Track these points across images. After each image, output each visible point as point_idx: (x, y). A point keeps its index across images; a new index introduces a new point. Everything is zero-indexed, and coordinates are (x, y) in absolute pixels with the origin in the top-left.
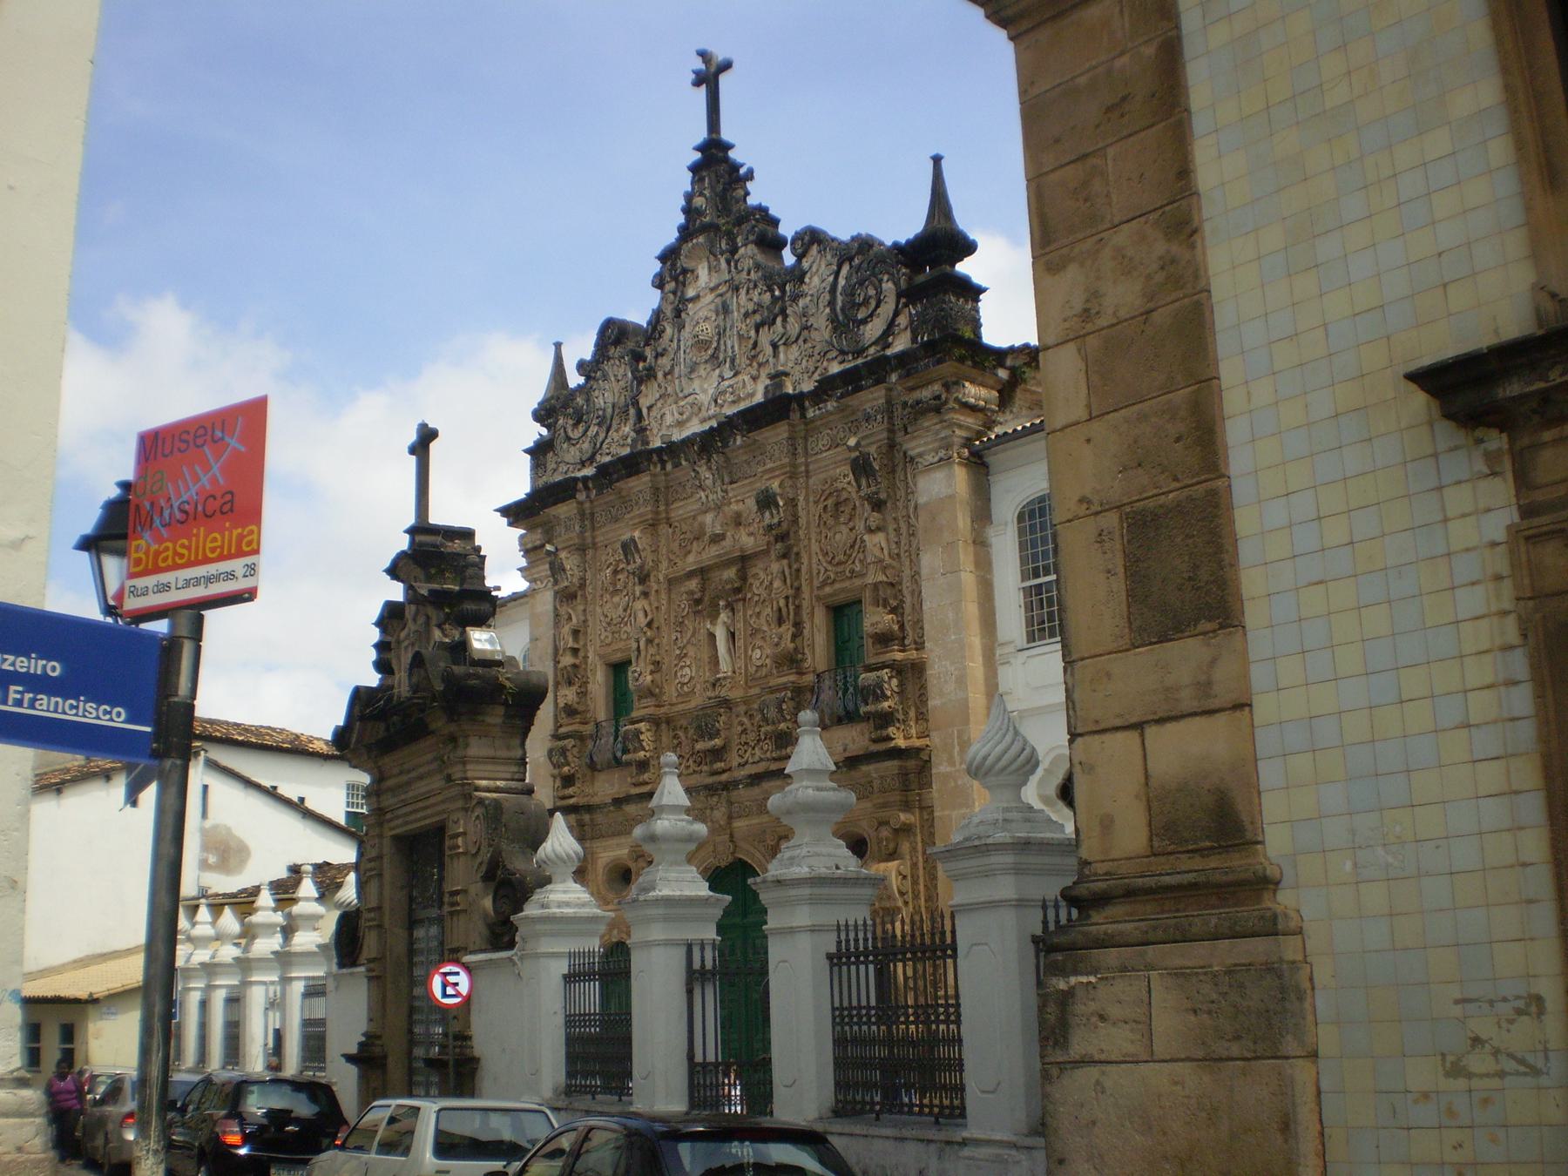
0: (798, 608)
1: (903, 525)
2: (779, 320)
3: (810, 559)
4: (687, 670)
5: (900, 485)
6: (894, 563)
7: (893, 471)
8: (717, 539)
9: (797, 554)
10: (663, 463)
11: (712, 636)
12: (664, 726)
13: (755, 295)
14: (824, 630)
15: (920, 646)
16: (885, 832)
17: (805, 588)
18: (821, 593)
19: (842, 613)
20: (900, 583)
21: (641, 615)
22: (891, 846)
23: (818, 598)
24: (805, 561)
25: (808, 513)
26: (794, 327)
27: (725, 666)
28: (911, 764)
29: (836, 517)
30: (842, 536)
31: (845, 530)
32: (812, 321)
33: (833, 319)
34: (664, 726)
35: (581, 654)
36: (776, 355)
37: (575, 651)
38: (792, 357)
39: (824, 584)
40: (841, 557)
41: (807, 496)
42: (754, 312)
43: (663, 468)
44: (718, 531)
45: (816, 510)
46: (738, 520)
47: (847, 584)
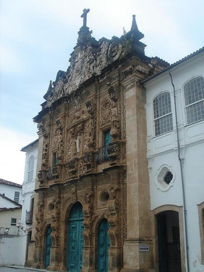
1: (122, 106)
2: (95, 61)
3: (99, 119)
4: (70, 152)
5: (122, 95)
6: (119, 116)
7: (120, 92)
8: (79, 117)
9: (96, 118)
10: (67, 101)
13: (90, 57)
14: (101, 137)
15: (125, 138)
16: (113, 191)
17: (97, 127)
19: (106, 132)
20: (121, 121)
22: (114, 195)
24: (98, 120)
25: (99, 107)
26: (98, 62)
27: (78, 151)
29: (106, 107)
30: (107, 111)
31: (107, 110)
32: (102, 59)
33: (107, 58)
34: (63, 167)
35: (48, 151)
36: (93, 70)
37: (46, 150)
38: (97, 69)
40: (107, 117)
41: (99, 103)
42: (90, 61)
43: (67, 102)
44: (78, 115)
45: (101, 106)
46: (83, 112)
47: (108, 124)
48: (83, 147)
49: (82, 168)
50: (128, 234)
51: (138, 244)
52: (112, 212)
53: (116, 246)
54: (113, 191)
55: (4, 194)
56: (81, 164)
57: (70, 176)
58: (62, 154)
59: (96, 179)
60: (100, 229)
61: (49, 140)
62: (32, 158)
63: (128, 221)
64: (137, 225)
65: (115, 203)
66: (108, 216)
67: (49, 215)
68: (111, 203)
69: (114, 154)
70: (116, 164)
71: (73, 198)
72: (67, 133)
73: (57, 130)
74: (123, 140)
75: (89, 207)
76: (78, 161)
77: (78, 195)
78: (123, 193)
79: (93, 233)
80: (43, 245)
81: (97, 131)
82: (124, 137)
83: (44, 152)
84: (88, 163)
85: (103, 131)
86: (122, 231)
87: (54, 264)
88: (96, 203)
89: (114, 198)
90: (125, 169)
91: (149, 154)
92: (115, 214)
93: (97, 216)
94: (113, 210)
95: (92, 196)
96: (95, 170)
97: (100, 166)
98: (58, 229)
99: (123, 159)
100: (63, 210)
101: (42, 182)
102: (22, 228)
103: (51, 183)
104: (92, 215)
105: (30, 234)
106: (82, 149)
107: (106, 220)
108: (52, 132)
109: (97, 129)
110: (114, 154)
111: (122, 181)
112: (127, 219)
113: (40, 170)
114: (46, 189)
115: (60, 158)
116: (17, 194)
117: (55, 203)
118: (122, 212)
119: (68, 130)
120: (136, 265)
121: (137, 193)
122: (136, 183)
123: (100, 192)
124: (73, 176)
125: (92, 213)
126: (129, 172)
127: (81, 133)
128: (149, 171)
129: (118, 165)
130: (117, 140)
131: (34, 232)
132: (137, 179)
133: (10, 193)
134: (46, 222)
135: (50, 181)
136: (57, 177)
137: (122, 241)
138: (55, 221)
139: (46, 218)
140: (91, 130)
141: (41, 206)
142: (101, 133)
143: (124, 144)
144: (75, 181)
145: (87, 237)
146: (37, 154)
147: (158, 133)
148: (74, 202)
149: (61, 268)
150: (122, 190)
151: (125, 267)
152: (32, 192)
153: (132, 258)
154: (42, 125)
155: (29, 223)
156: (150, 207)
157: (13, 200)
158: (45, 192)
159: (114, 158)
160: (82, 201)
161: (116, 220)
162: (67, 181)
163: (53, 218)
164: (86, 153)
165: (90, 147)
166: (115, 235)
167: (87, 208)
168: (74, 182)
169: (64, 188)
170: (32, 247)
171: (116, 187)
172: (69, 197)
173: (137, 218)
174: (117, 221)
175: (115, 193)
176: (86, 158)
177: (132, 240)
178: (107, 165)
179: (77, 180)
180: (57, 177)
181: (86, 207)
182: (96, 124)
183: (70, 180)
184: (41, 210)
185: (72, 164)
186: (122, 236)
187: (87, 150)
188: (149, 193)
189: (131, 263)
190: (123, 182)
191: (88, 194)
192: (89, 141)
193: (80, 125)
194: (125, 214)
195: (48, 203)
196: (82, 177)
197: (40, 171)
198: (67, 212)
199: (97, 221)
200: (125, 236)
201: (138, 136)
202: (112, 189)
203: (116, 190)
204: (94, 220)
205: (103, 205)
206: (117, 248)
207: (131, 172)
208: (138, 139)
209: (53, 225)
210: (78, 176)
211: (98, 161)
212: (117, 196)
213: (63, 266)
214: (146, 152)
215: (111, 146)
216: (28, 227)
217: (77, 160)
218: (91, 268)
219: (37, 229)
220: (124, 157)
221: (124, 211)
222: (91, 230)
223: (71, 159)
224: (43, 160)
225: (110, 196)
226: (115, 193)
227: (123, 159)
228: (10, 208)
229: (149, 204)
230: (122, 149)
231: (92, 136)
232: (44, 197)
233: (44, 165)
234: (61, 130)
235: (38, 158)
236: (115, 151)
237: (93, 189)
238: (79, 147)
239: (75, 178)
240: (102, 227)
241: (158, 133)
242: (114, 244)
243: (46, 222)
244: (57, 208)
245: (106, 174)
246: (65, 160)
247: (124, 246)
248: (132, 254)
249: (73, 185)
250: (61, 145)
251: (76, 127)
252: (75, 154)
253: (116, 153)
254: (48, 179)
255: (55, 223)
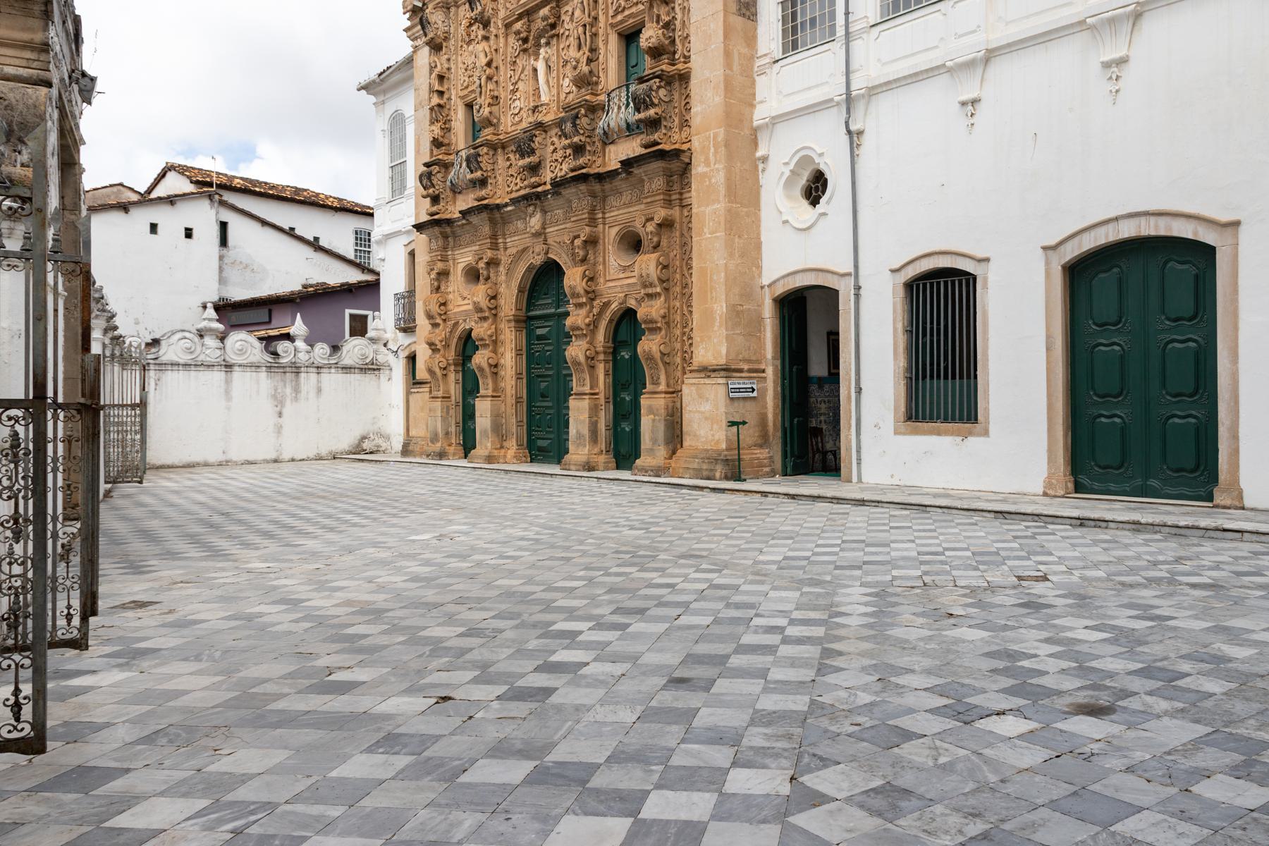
0: (595, 35)
4: (517, 103)
11: (535, 70)
12: (500, 151)
14: (615, 54)
15: (687, 59)
17: (602, 18)
18: (615, 21)
19: (630, 37)
21: (482, 55)
22: (655, 239)
23: (612, 25)
27: (544, 98)
28: (675, 165)
34: (500, 151)
39: (617, 13)
47: (634, 10)
48: (560, 86)
49: (560, 153)
50: (695, 352)
51: (722, 381)
52: (650, 291)
53: (662, 387)
54: (650, 227)
55: (316, 239)
56: (555, 139)
57: (523, 180)
58: (495, 109)
59: (603, 191)
60: (619, 339)
61: (449, 60)
62: (397, 121)
63: (695, 316)
64: (720, 326)
65: (658, 263)
66: (639, 301)
67: (464, 299)
68: (648, 264)
69: (652, 112)
70: (659, 144)
71: (537, 250)
72: (507, 36)
73: (471, 25)
74: (680, 66)
75: (584, 276)
76: (546, 132)
77: (550, 241)
78: (682, 235)
79: (597, 353)
80: (453, 392)
81: (601, 32)
82: (685, 57)
83: (436, 100)
84: (576, 139)
85: (619, 34)
86: (678, 346)
87: (489, 445)
88: (604, 263)
89: (656, 247)
90: (687, 160)
91: (760, 114)
92: (659, 294)
93: (606, 305)
94: (651, 285)
95: (592, 242)
96: (599, 162)
97: (612, 148)
98: (495, 343)
99: (681, 130)
100: (508, 287)
101: (435, 199)
102: (385, 345)
103: (466, 201)
104: (593, 300)
105: (412, 359)
106: (554, 91)
107: (635, 312)
108: (456, 29)
109: (602, 24)
110: (652, 112)
111: (677, 196)
112: (694, 309)
113: (427, 159)
114: (449, 222)
115: (488, 123)
116: (363, 239)
117: (481, 265)
118: (678, 289)
119: (508, 26)
120: (717, 437)
121: (721, 234)
122: (719, 202)
123: (614, 231)
124: (533, 180)
125: (592, 295)
126: (698, 169)
127: (552, 37)
128: (761, 166)
129: (667, 147)
130: (664, 67)
131: (423, 354)
132: (722, 191)
133: (339, 234)
134: (456, 324)
135: (460, 197)
136: (483, 182)
137: (679, 374)
138: (485, 319)
139: (457, 310)
140: (581, 29)
141: (439, 274)
142: (613, 40)
143: (684, 78)
144: (538, 196)
145: (579, 364)
146: (410, 104)
147: (792, 42)
148: (538, 260)
149: (511, 453)
150: (677, 225)
151: (686, 444)
152: (408, 232)
153: (706, 419)
154: (420, 5)
155: (407, 327)
156: (760, 275)
157: (351, 256)
158: (448, 230)
159: (654, 124)
160: (563, 260)
161: (662, 312)
162: (514, 195)
163: (478, 309)
164: (567, 108)
165: (579, 87)
166: (658, 356)
167: (578, 280)
168: (533, 199)
169: (506, 221)
170: (421, 396)
171: (661, 214)
172: (524, 243)
173: (720, 308)
174: (664, 317)
175: (659, 234)
176: (569, 125)
177: (707, 371)
178: (631, 148)
179: (545, 193)
180: (483, 182)
181: (573, 278)
182: (595, 8)
183: (523, 192)
184: (438, 288)
185: (524, 145)
186: (678, 360)
187: (571, 97)
188: (759, 234)
189: (702, 433)
190: (681, 199)
191: (578, 236)
192: (575, 68)
193: (545, 11)
194: (687, 297)
195: (461, 267)
196: (558, 185)
197: (427, 165)
198: (520, 291)
199: (608, 315)
200: (687, 361)
201: (727, 54)
202: (648, 220)
203: (659, 225)
204: (600, 314)
205: (625, 269)
206: (666, 393)
207: (705, 169)
208: (728, 64)
209: (481, 331)
210: (548, 180)
211: (605, 133)
212: (664, 243)
213: (515, 447)
214: (752, 106)
215: (644, 86)
216: (404, 340)
217: (540, 126)
218: (596, 450)
219: (431, 344)
220: (685, 123)
221: (685, 286)
222: (591, 343)
223: (524, 125)
224: (433, 127)
225: (645, 243)
226: (659, 234)
227: (681, 130)
228: (342, 285)
229: (759, 267)
230: (676, 96)
231: (586, 49)
232: (445, 248)
233: (437, 143)
234: (486, 24)
235: (418, 122)
236: (656, 101)
237: (592, 222)
238: (543, 84)
239: (540, 185)
240: (623, 336)
241: (792, 42)
242: (656, 383)
243: (456, 324)
244: (488, 278)
245: (630, 173)
246: (506, 126)
247: (684, 387)
248: (706, 407)
249: (532, 208)
250: (489, 78)
251: (535, 16)
252: (535, 109)
253: (657, 110)
254: (455, 190)
255: (486, 325)
